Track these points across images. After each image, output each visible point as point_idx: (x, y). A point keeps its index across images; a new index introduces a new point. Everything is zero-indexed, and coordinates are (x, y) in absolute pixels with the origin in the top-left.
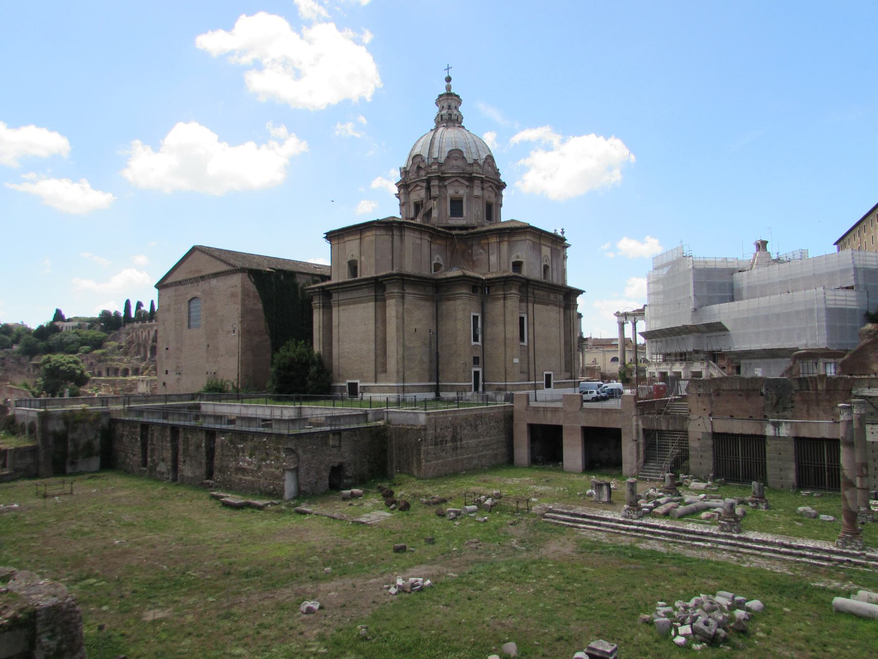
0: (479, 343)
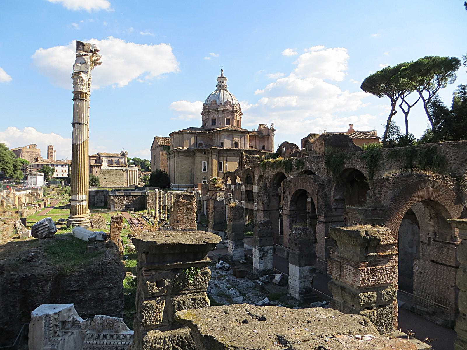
0: (206, 171)
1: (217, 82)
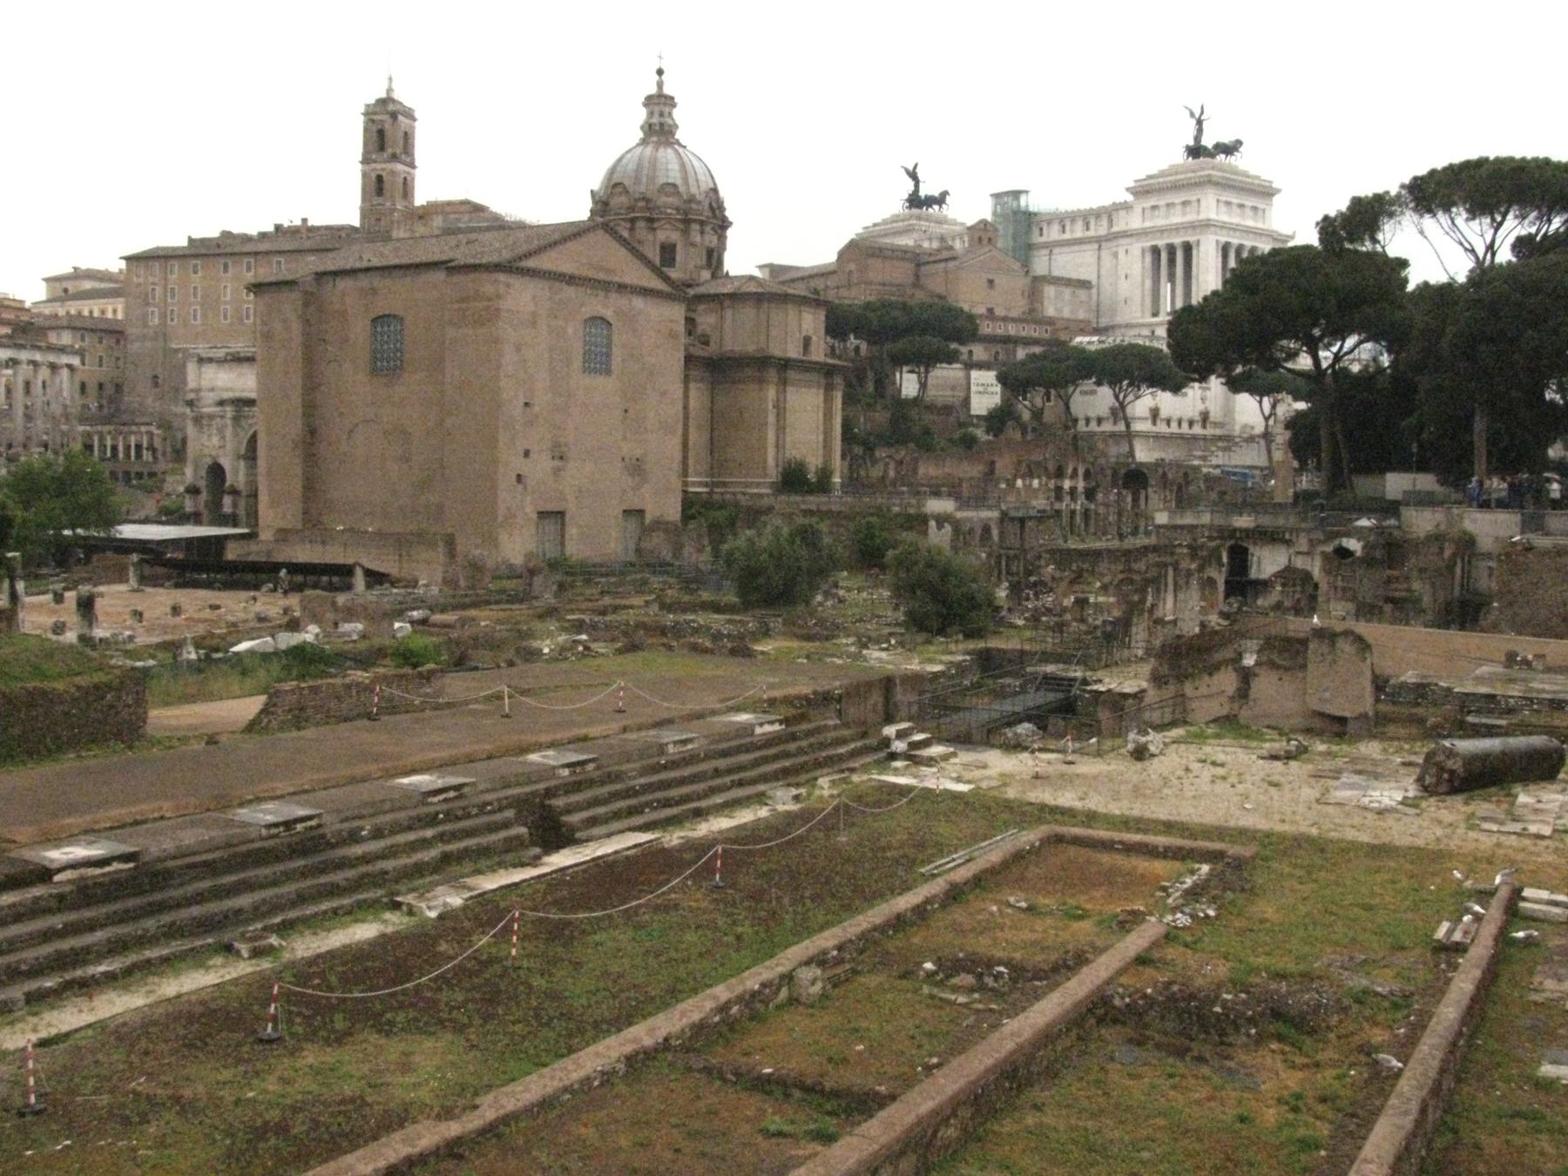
1: (641, 114)
